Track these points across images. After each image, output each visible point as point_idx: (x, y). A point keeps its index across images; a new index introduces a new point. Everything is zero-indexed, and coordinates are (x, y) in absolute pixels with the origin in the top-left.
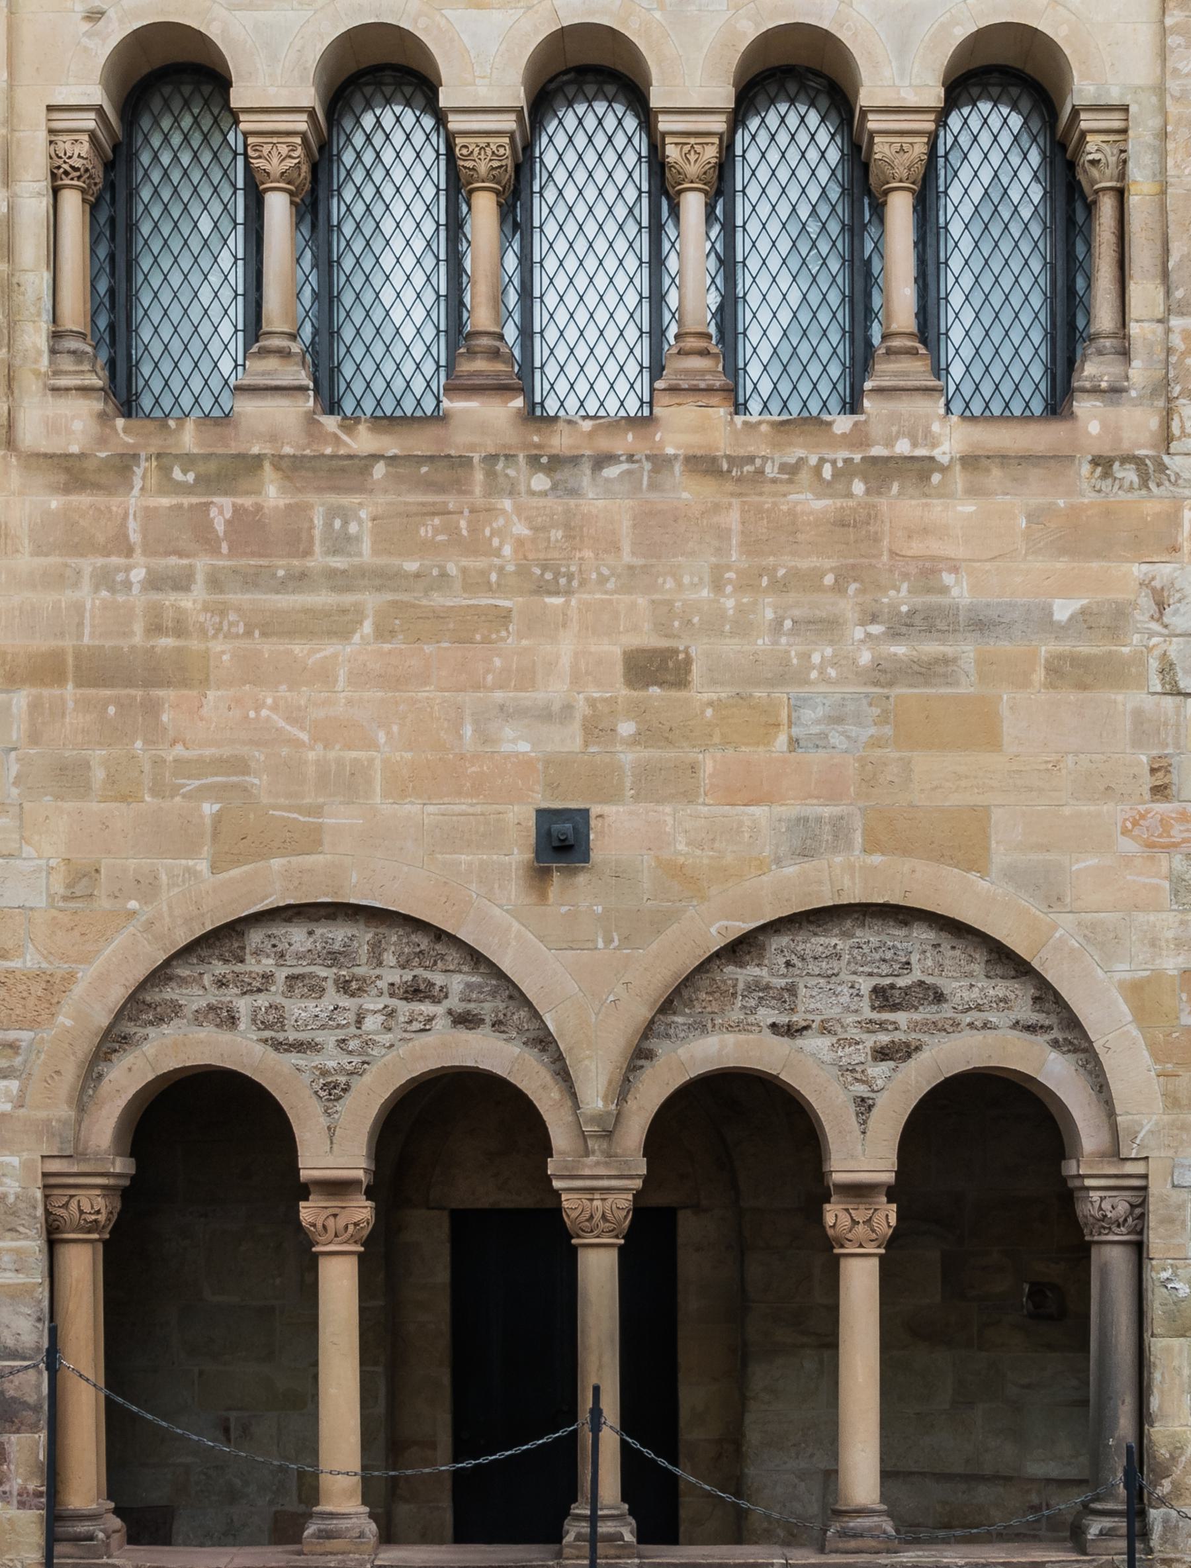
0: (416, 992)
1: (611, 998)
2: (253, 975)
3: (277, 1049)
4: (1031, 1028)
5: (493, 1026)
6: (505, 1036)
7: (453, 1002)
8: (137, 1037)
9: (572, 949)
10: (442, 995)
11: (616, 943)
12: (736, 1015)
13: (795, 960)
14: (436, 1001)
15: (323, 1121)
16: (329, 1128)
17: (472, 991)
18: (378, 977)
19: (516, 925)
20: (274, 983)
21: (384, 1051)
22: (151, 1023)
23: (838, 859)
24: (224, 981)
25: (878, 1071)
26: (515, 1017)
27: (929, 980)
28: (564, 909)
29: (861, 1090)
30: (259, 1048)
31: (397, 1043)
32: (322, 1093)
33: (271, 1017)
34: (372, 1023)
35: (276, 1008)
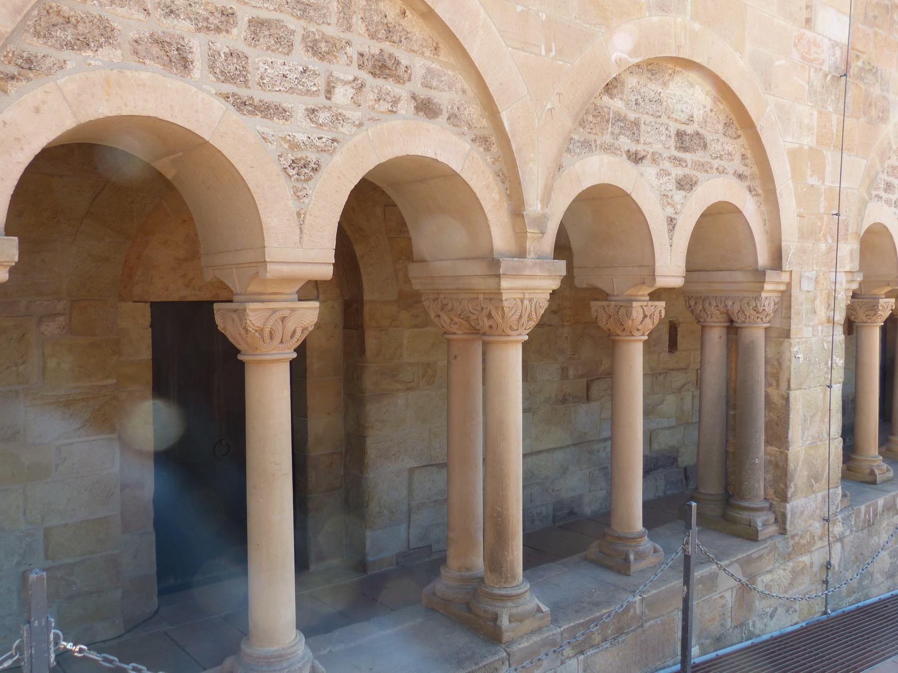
0: (383, 67)
1: (549, 106)
2: (209, 7)
3: (239, 109)
4: (741, 177)
5: (449, 118)
6: (455, 129)
7: (415, 86)
8: (48, 62)
9: (524, 51)
10: (406, 76)
11: (553, 53)
12: (608, 138)
13: (640, 101)
14: (399, 80)
15: (291, 204)
16: (299, 214)
17: (432, 77)
18: (348, 43)
19: (483, 14)
20: (235, 24)
21: (354, 129)
22: (71, 46)
23: (679, 20)
24: (174, 8)
25: (678, 196)
26: (466, 112)
27: (701, 131)
28: (519, 8)
29: (670, 211)
30: (218, 105)
31: (366, 123)
32: (292, 172)
33: (232, 68)
34: (342, 95)
35: (238, 57)
